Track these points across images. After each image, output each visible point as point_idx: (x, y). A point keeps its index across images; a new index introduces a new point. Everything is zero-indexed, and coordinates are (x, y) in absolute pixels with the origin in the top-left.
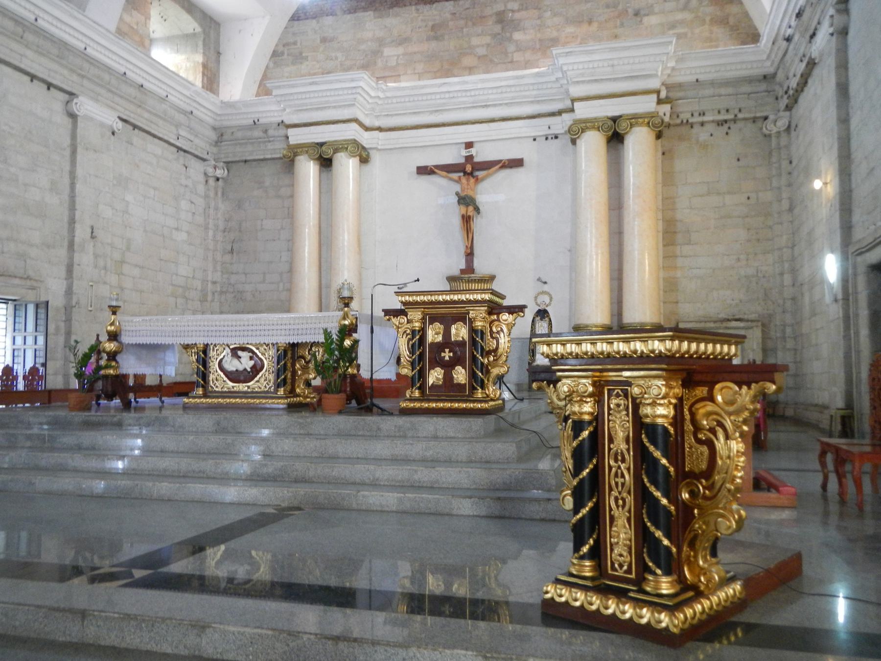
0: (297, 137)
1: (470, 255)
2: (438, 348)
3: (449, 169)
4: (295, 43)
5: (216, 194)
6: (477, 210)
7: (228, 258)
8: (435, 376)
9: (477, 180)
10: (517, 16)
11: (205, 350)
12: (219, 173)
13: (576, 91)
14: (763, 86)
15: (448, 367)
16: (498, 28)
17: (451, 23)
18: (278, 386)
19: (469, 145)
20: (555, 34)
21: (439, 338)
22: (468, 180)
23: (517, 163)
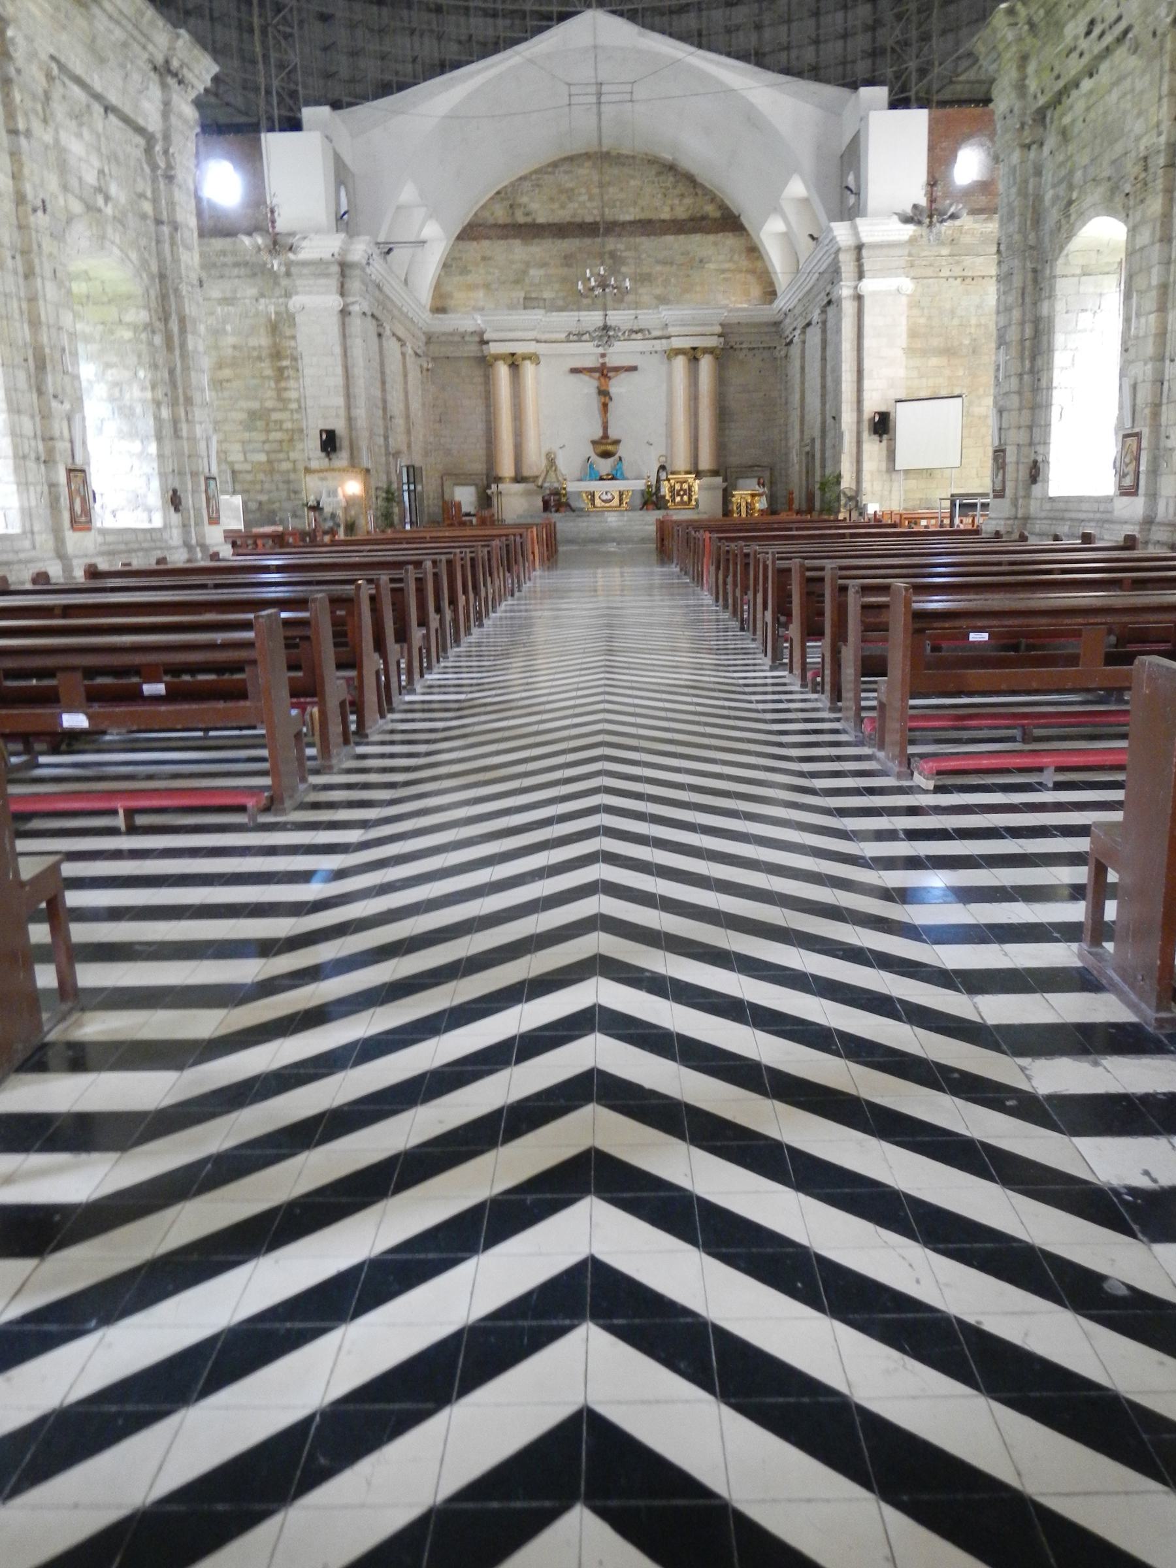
0: (494, 349)
1: (605, 428)
2: (679, 491)
3: (590, 370)
4: (461, 259)
6: (611, 399)
7: (437, 426)
8: (678, 499)
9: (610, 378)
10: (624, 254)
13: (672, 330)
14: (774, 329)
15: (682, 496)
20: (648, 270)
23: (634, 369)
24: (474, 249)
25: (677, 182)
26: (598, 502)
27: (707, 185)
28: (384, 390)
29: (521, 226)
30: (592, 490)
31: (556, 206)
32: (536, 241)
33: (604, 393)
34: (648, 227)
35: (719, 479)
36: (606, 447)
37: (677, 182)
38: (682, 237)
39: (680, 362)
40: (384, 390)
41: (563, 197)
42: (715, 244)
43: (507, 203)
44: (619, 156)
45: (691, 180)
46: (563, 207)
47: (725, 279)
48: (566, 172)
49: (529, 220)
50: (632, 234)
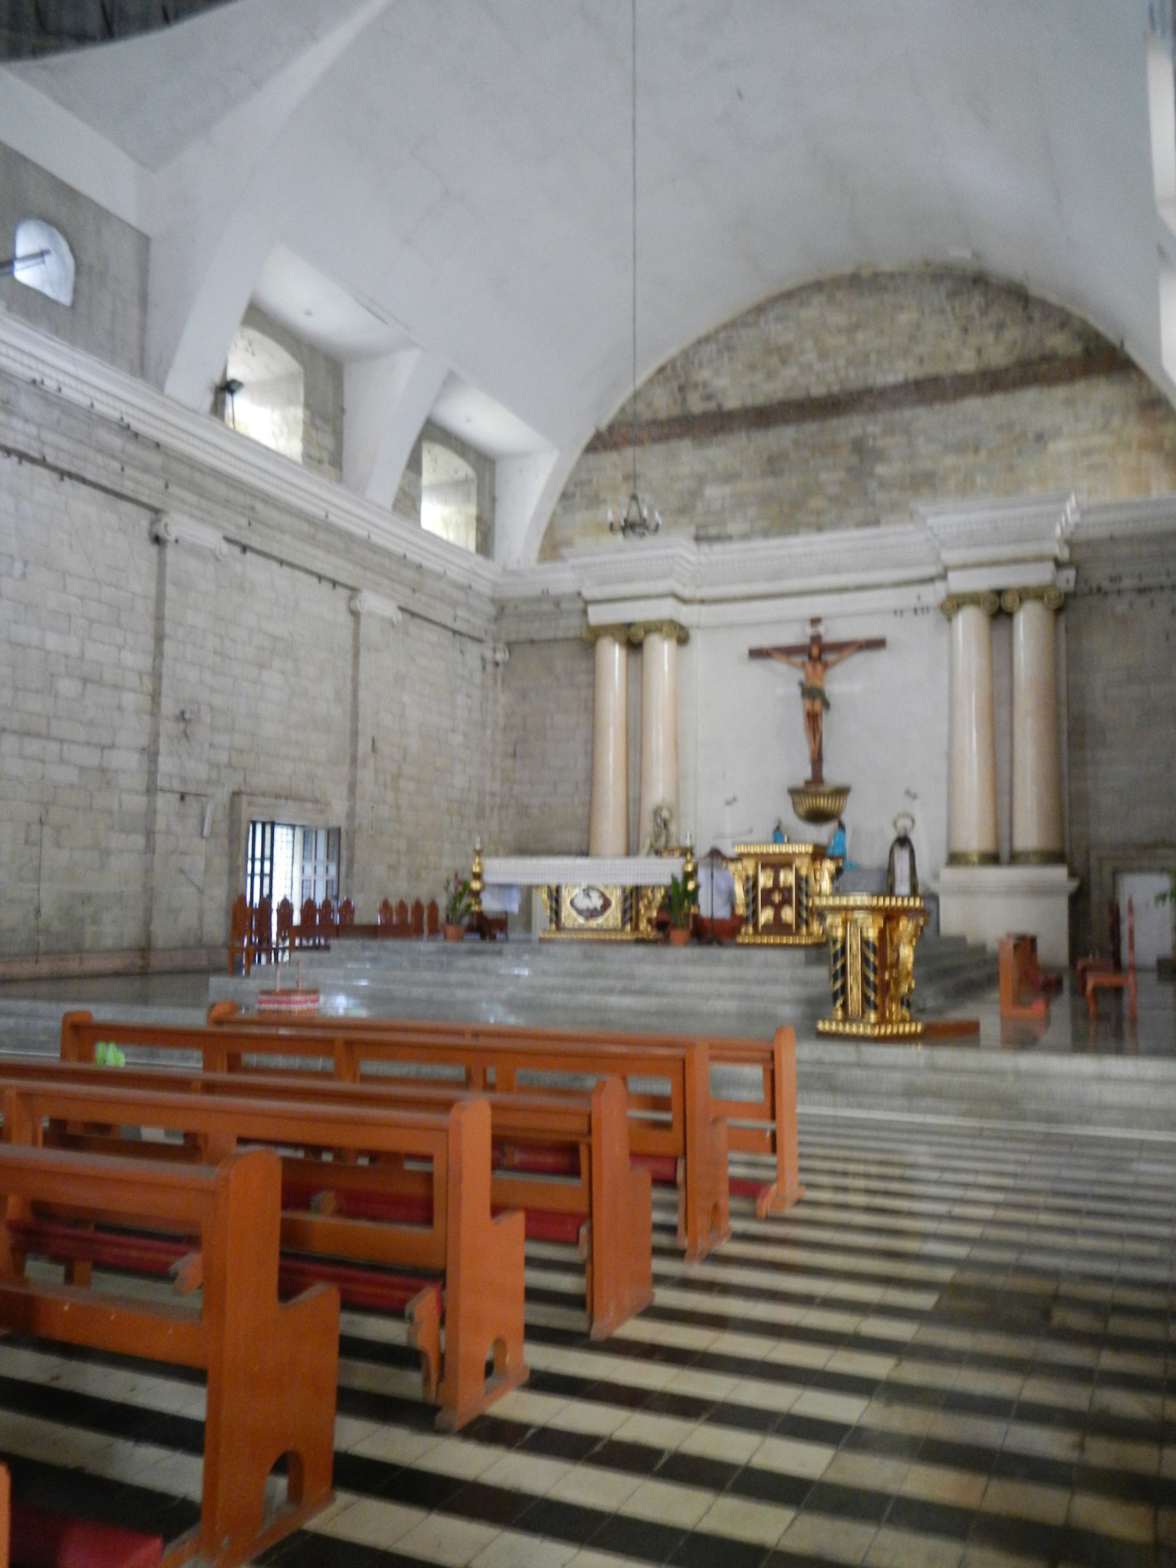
0: (599, 615)
1: (817, 760)
2: (768, 893)
3: (788, 652)
5: (496, 683)
6: (826, 704)
7: (509, 762)
8: (766, 915)
9: (826, 666)
10: (880, 443)
11: (558, 889)
12: (500, 656)
13: (950, 556)
15: (778, 908)
16: (854, 460)
17: (792, 455)
18: (624, 923)
19: (815, 621)
21: (770, 884)
22: (814, 668)
23: (877, 644)
24: (611, 463)
25: (988, 305)
26: (568, 915)
27: (1052, 298)
28: (158, 653)
29: (695, 418)
30: (553, 882)
31: (758, 377)
32: (721, 437)
33: (813, 694)
34: (930, 390)
35: (1059, 874)
36: (818, 801)
37: (988, 305)
38: (998, 399)
39: (969, 621)
40: (158, 653)
41: (774, 361)
42: (1069, 402)
43: (675, 385)
44: (876, 275)
45: (1018, 297)
46: (771, 375)
47: (1092, 468)
48: (778, 319)
49: (711, 406)
50: (895, 405)
